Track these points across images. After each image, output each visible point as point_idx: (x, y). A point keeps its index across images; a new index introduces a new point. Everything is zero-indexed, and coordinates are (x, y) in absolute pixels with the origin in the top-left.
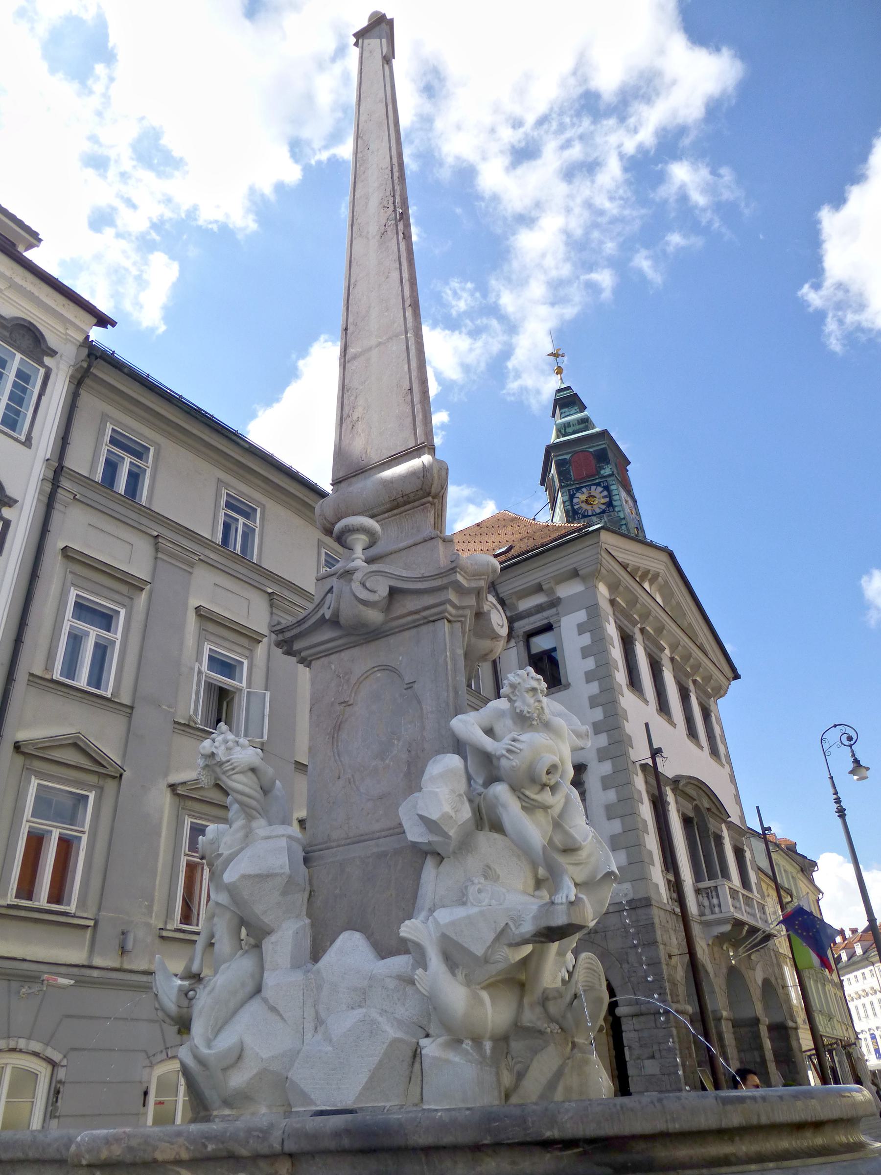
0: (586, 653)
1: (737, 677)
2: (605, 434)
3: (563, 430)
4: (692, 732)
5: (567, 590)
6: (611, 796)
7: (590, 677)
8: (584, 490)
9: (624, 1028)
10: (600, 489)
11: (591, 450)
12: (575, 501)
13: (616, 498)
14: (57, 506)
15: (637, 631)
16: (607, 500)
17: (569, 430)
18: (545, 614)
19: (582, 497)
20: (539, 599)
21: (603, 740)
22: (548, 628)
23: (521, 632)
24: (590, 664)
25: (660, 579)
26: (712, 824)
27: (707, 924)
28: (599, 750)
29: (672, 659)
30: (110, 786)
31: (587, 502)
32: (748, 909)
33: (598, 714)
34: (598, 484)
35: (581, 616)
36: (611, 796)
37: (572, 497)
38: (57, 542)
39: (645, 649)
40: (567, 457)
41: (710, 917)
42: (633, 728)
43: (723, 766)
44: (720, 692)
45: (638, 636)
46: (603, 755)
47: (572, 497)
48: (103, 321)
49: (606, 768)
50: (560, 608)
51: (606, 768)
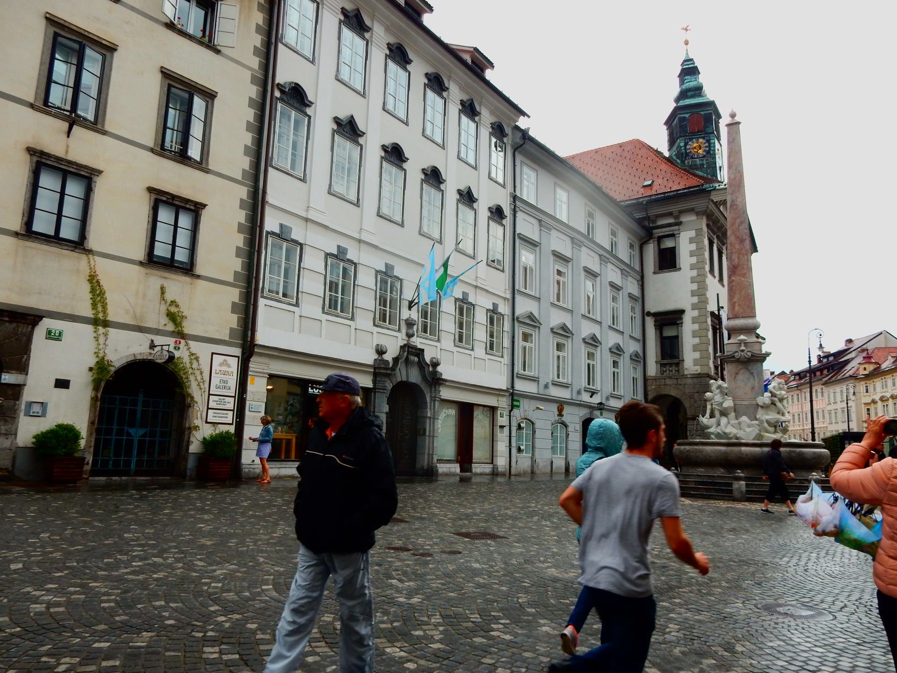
0: (692, 254)
2: (712, 104)
3: (683, 95)
6: (696, 327)
7: (692, 267)
12: (688, 147)
15: (715, 237)
17: (690, 94)
18: (672, 228)
20: (671, 221)
21: (695, 300)
22: (673, 235)
24: (694, 260)
28: (693, 304)
30: (537, 330)
33: (695, 287)
34: (703, 138)
35: (692, 233)
36: (696, 327)
37: (686, 144)
40: (687, 116)
45: (715, 241)
47: (686, 144)
48: (523, 114)
49: (696, 313)
51: (696, 313)
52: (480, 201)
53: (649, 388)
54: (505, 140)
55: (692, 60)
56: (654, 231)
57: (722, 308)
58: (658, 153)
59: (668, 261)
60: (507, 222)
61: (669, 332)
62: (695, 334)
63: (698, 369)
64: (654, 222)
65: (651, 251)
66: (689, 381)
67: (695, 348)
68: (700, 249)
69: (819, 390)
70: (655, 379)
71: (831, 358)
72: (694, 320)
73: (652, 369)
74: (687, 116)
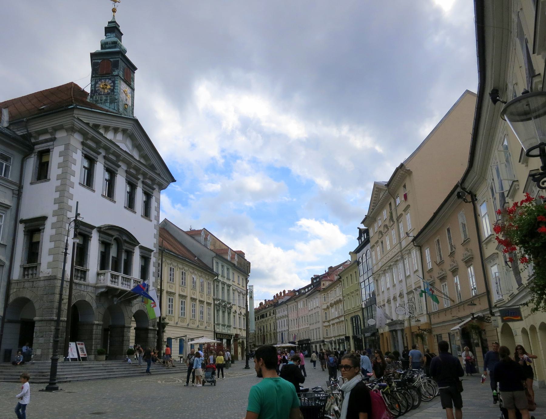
0: (60, 166)
1: (174, 181)
4: (131, 205)
5: (60, 135)
8: (103, 81)
9: (36, 325)
10: (110, 82)
11: (112, 60)
12: (97, 85)
13: (116, 88)
16: (112, 88)
18: (48, 144)
19: (101, 85)
20: (48, 137)
21: (56, 207)
23: (37, 150)
24: (60, 171)
25: (128, 132)
26: (125, 247)
27: (96, 288)
29: (126, 171)
31: (103, 88)
32: (124, 282)
34: (110, 79)
35: (62, 148)
36: (53, 232)
37: (96, 83)
39: (104, 166)
40: (99, 61)
41: (99, 285)
42: (72, 203)
43: (151, 221)
44: (162, 187)
46: (55, 214)
47: (96, 83)
49: (54, 219)
50: (55, 143)
53: (12, 291)
56: (36, 147)
57: (79, 214)
59: (42, 174)
62: (52, 239)
64: (35, 138)
65: (31, 163)
66: (42, 284)
67: (50, 253)
69: (305, 302)
70: (18, 282)
71: (318, 280)
72: (53, 226)
73: (17, 274)
74: (99, 61)
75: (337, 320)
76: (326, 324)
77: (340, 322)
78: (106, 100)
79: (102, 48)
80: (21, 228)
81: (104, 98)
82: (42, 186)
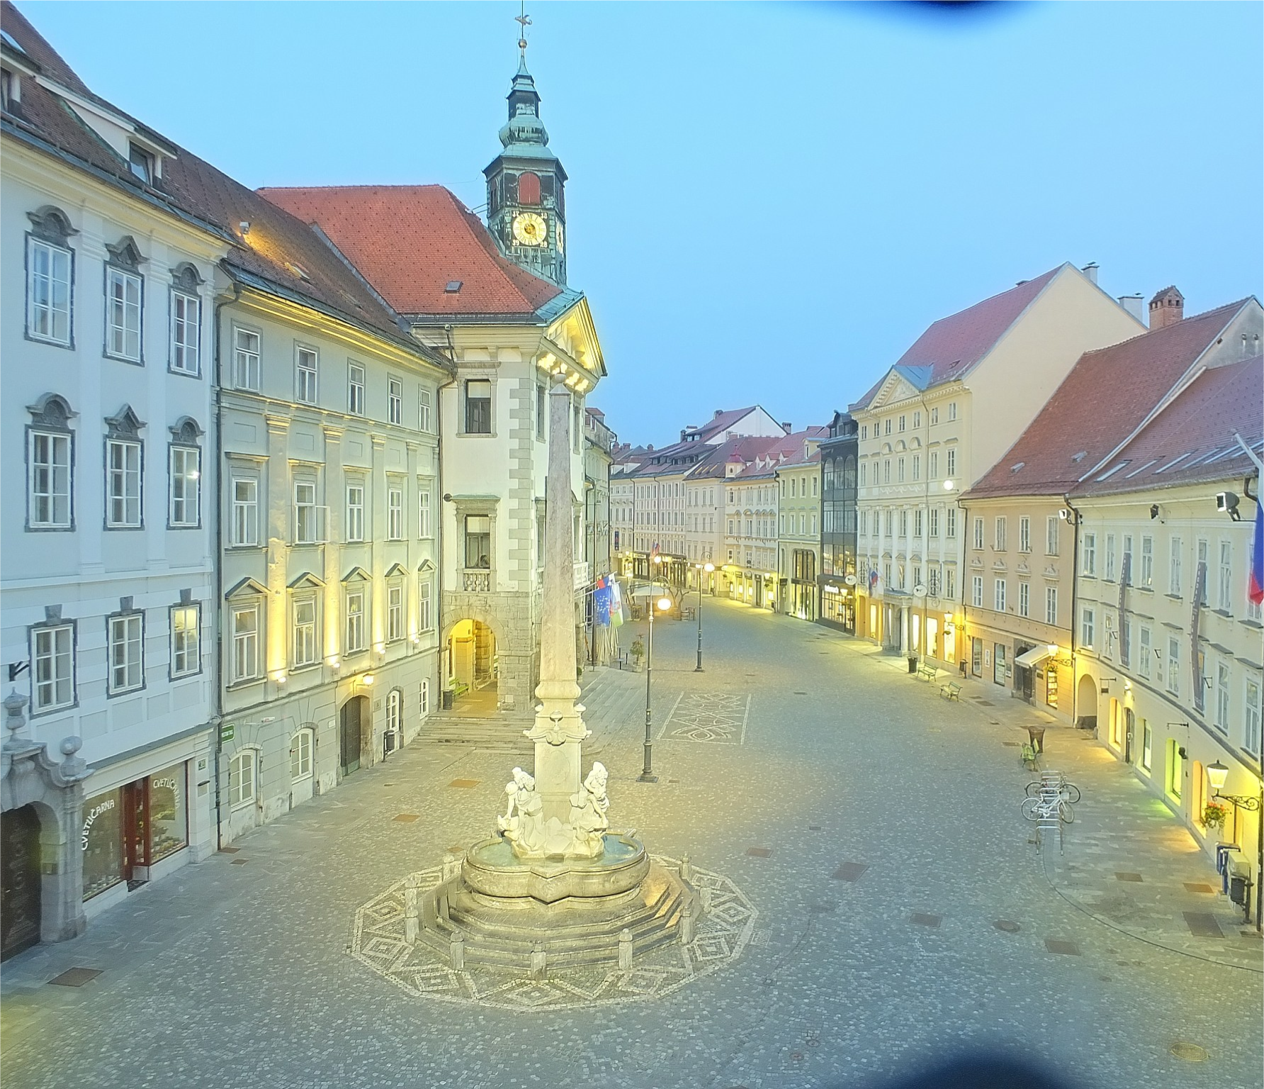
0: (513, 414)
7: (513, 434)
14: (223, 421)
21: (515, 484)
28: (510, 490)
35: (515, 383)
38: (225, 449)
40: (517, 173)
49: (514, 504)
51: (514, 504)
52: (151, 425)
53: (446, 609)
54: (199, 290)
55: (530, 78)
58: (472, 219)
59: (478, 417)
60: (206, 441)
61: (475, 525)
63: (514, 586)
67: (511, 554)
68: (525, 408)
73: (451, 582)
75: (760, 544)
76: (731, 541)
77: (765, 549)
78: (535, 257)
79: (511, 138)
80: (449, 507)
81: (531, 253)
82: (477, 441)
